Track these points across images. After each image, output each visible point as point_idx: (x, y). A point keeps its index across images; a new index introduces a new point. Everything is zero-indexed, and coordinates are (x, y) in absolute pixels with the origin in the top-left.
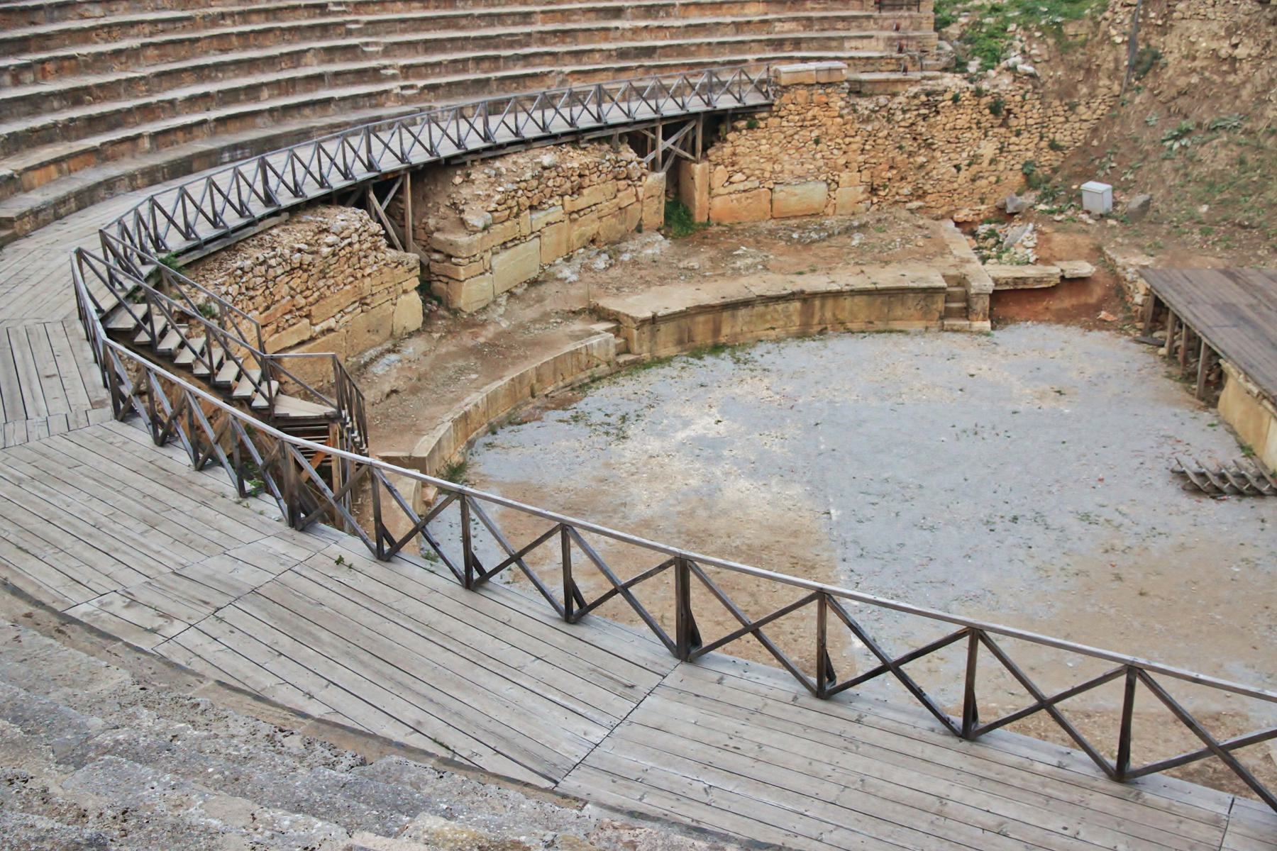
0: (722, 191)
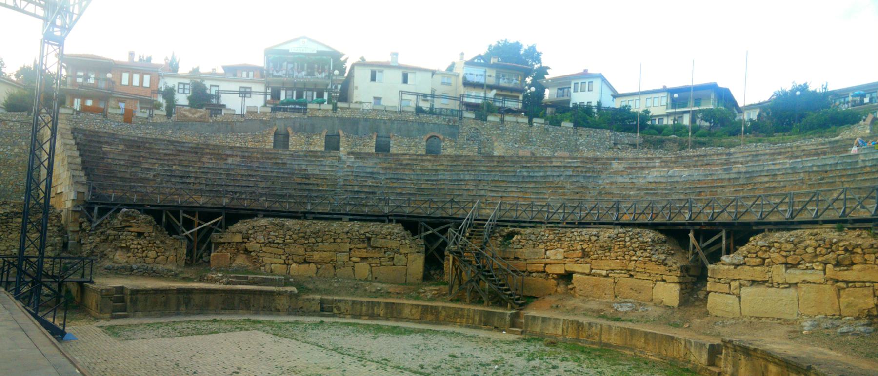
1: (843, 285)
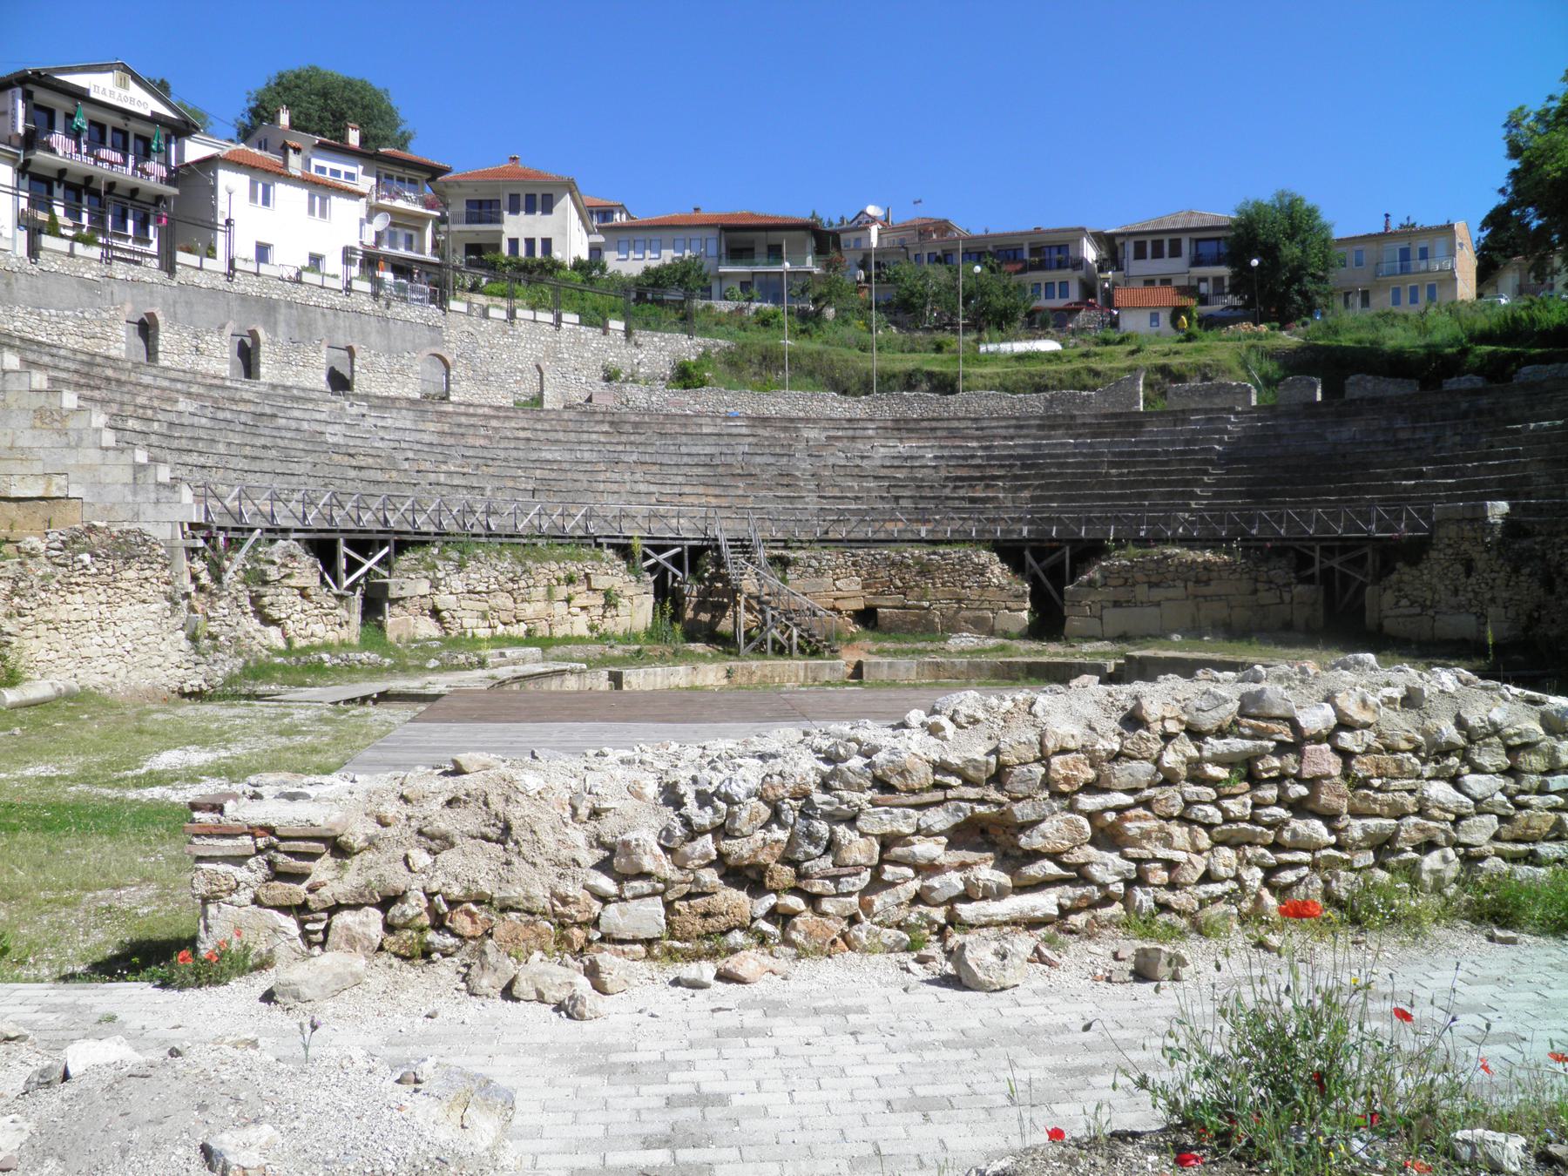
0: (1390, 613)
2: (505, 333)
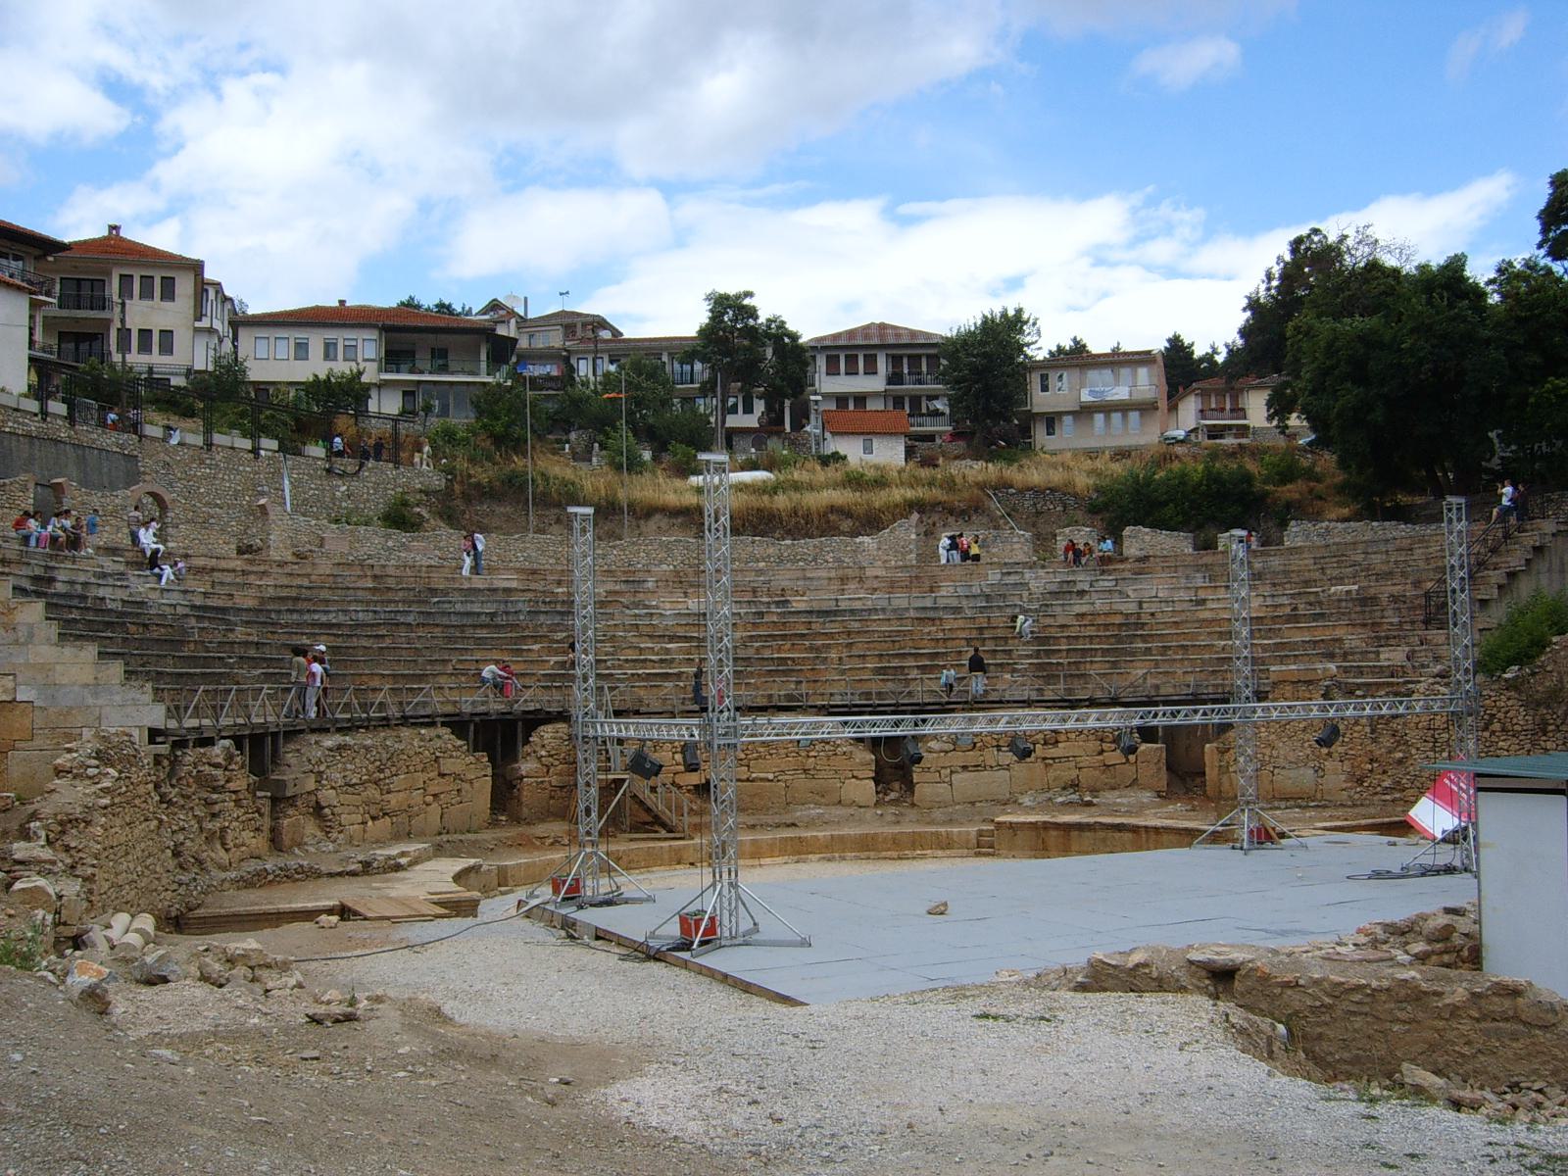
1: (1051, 762)
2: (202, 462)
